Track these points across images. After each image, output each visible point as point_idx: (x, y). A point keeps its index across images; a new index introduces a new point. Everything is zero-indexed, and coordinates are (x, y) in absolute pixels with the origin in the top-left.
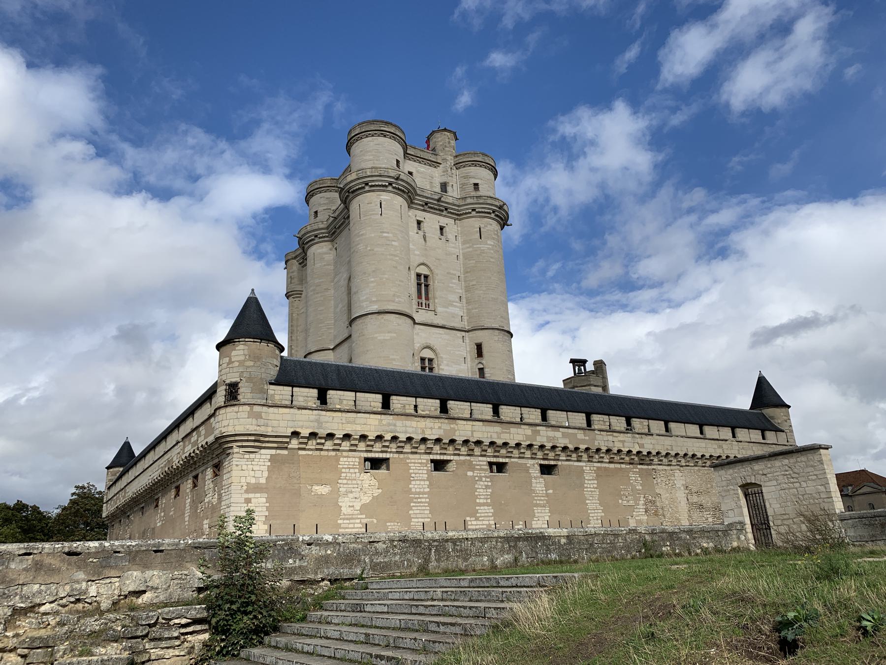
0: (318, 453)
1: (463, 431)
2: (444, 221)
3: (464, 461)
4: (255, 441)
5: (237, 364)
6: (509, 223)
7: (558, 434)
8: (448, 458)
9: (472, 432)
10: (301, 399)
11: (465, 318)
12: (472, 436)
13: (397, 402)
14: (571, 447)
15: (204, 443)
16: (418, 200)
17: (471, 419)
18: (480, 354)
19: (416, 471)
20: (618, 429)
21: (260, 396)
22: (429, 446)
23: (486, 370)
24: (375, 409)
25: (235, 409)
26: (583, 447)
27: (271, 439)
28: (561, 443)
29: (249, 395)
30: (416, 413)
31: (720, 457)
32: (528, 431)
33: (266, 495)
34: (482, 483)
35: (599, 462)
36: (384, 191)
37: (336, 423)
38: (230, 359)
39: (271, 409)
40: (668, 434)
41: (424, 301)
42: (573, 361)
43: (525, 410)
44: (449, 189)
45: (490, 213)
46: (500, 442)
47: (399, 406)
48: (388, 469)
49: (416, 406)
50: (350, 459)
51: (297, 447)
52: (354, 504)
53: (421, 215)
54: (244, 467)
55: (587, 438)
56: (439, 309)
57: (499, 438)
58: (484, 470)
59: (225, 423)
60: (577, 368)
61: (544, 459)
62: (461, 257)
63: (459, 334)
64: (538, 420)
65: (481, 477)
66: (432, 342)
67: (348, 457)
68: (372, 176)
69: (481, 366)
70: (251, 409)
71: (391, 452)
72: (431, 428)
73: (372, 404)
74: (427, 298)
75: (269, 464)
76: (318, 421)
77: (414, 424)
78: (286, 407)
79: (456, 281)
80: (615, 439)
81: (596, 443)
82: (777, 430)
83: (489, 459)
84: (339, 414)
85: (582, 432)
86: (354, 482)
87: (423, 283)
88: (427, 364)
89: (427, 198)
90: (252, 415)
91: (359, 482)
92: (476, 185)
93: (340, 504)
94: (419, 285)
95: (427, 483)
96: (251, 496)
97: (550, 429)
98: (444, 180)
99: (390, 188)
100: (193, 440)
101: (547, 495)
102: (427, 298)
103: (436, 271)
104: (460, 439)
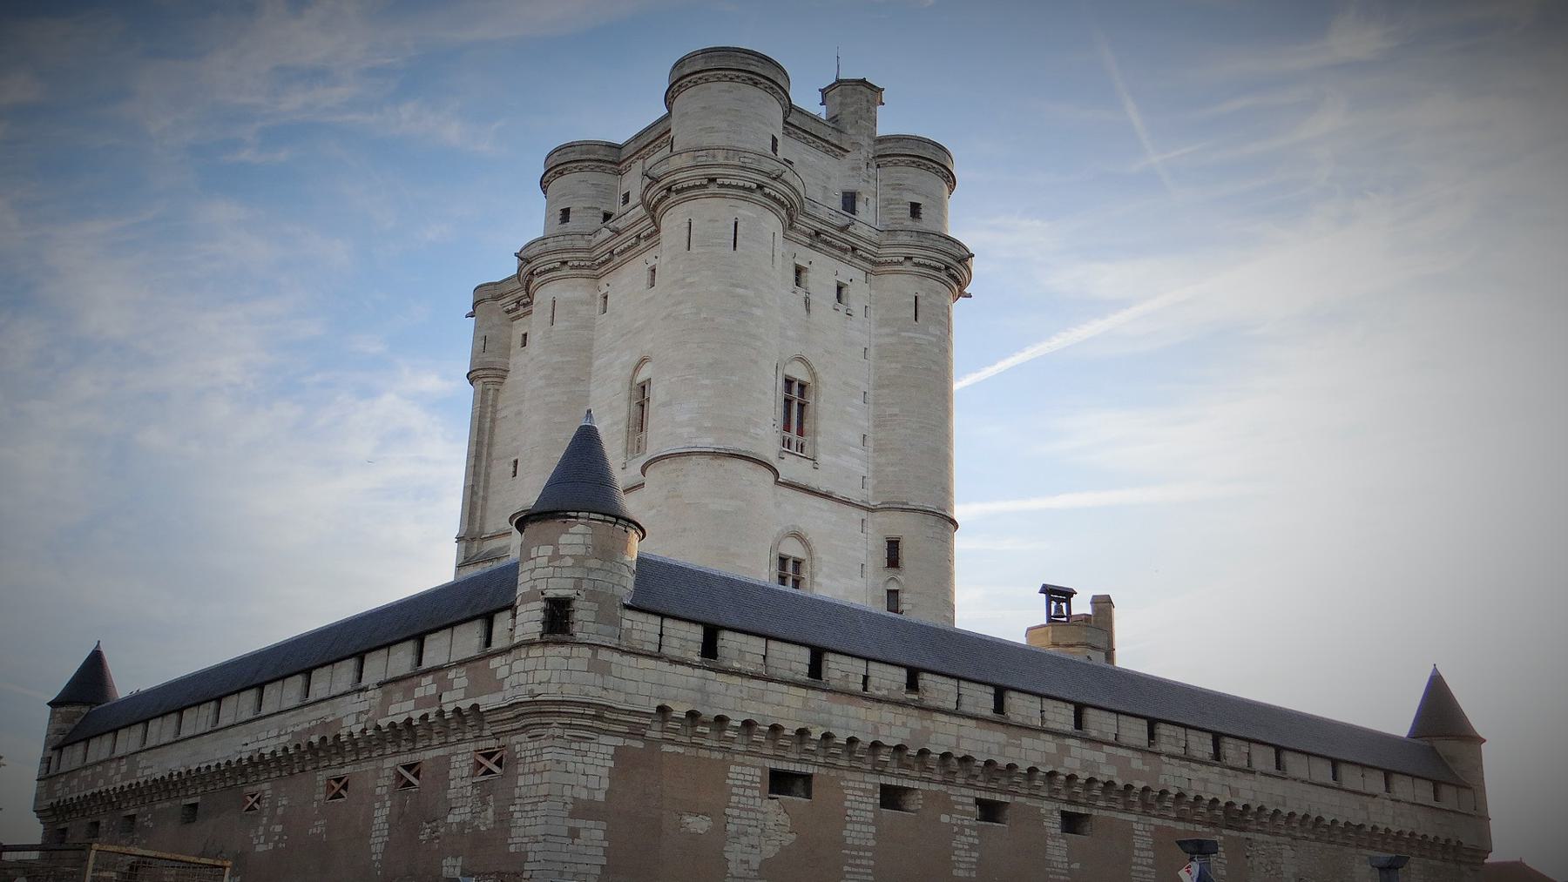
0: (692, 752)
1: (945, 735)
2: (849, 273)
3: (937, 793)
4: (595, 717)
5: (570, 562)
6: (967, 290)
7: (1099, 756)
8: (906, 783)
9: (959, 738)
10: (675, 643)
11: (871, 482)
12: (958, 746)
14: (1120, 783)
15: (465, 705)
16: (804, 223)
17: (956, 713)
18: (893, 561)
19: (855, 805)
20: (1199, 755)
21: (609, 629)
22: (882, 758)
23: (903, 597)
24: (798, 677)
25: (565, 650)
26: (1139, 785)
27: (622, 717)
28: (1106, 772)
29: (592, 627)
30: (864, 694)
31: (1361, 826)
32: (1048, 745)
33: (604, 825)
34: (964, 839)
35: (1159, 816)
36: (745, 199)
37: (730, 698)
38: (556, 551)
39: (627, 658)
40: (1279, 773)
41: (793, 435)
42: (1049, 591)
44: (860, 206)
45: (939, 269)
46: (1002, 762)
47: (838, 674)
48: (808, 796)
49: (866, 678)
50: (747, 770)
51: (659, 735)
52: (751, 857)
53: (805, 256)
54: (571, 767)
55: (1147, 768)
56: (823, 458)
57: (1001, 754)
58: (969, 814)
59: (541, 675)
60: (1054, 604)
61: (1069, 802)
62: (872, 352)
63: (857, 514)
64: (1069, 727)
65: (962, 827)
66: (805, 525)
67: (742, 764)
68: (726, 166)
69: (893, 587)
70: (595, 655)
71: (815, 764)
72: (890, 725)
73: (795, 666)
74: (801, 432)
75: (612, 764)
76: (701, 690)
77: (862, 712)
78: (650, 656)
79: (859, 402)
80: (1193, 775)
81: (1161, 781)
82: (1460, 786)
83: (978, 794)
84: (737, 680)
85: (1138, 755)
86: (752, 815)
87: (796, 401)
89: (822, 222)
91: (760, 816)
92: (915, 210)
93: (727, 855)
94: (788, 402)
95: (873, 829)
96: (580, 823)
97: (1087, 745)
99: (758, 196)
100: (419, 693)
101: (1070, 870)
102: (801, 432)
103: (821, 375)
104: (937, 750)
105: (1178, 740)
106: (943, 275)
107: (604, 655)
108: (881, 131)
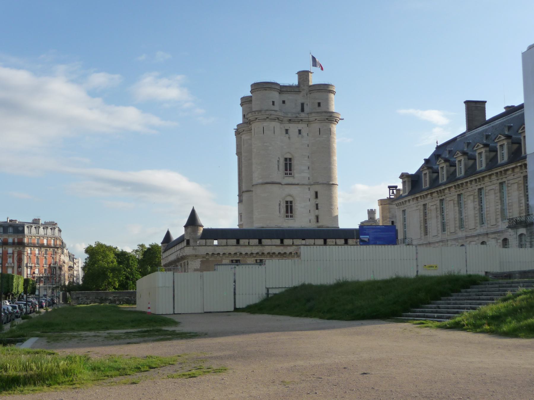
2: (301, 126)
13: (242, 242)
18: (317, 197)
42: (390, 187)
43: (295, 240)
44: (305, 106)
46: (282, 252)
53: (287, 126)
56: (296, 175)
63: (307, 187)
79: (306, 159)
88: (289, 204)
90: (194, 249)
92: (319, 104)
94: (286, 164)
98: (303, 101)
99: (267, 120)
102: (290, 170)
105: (333, 242)
106: (327, 121)
107: (195, 247)
108: (311, 84)
